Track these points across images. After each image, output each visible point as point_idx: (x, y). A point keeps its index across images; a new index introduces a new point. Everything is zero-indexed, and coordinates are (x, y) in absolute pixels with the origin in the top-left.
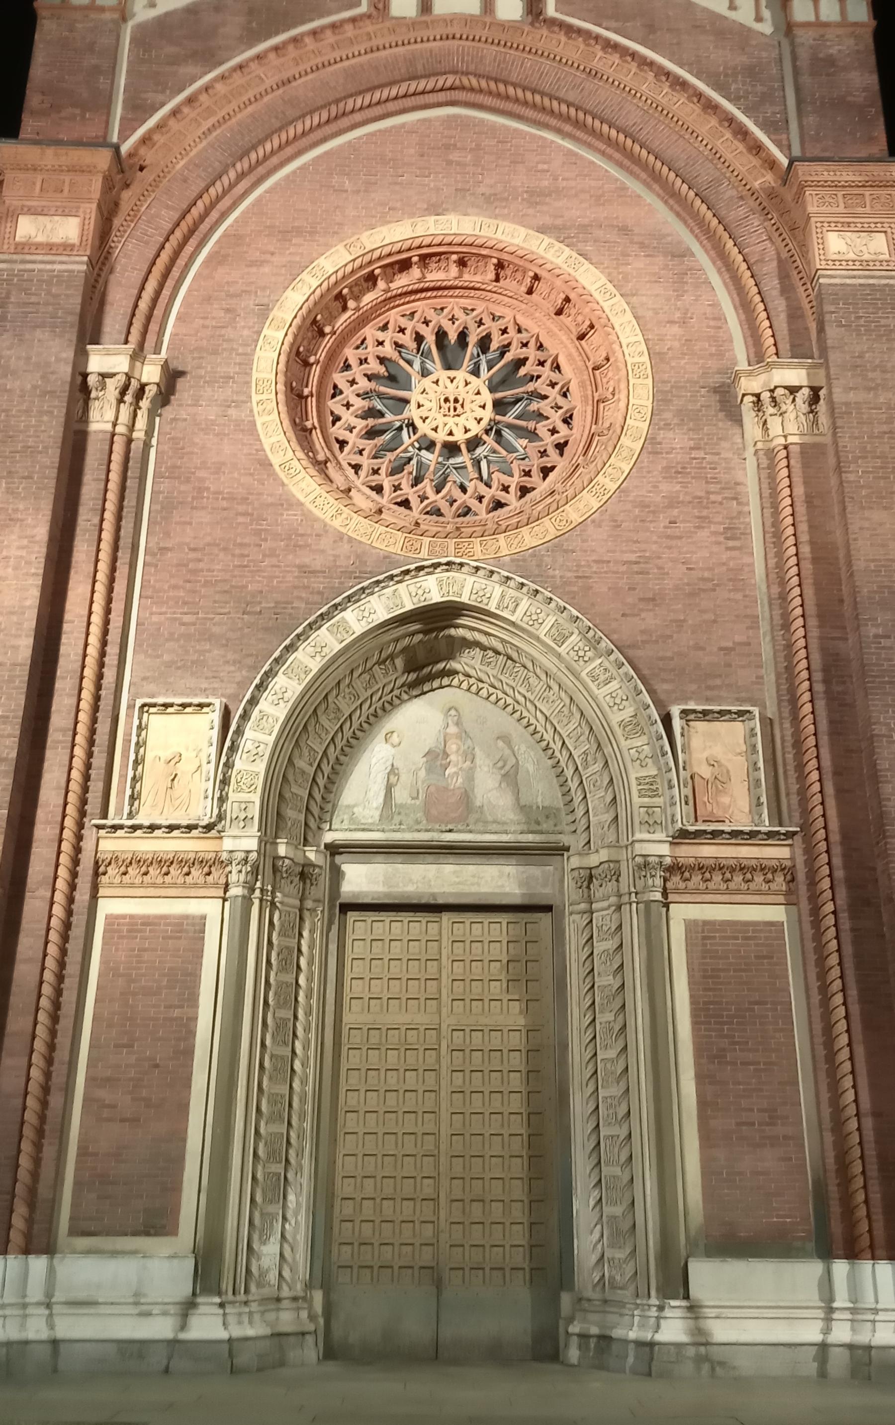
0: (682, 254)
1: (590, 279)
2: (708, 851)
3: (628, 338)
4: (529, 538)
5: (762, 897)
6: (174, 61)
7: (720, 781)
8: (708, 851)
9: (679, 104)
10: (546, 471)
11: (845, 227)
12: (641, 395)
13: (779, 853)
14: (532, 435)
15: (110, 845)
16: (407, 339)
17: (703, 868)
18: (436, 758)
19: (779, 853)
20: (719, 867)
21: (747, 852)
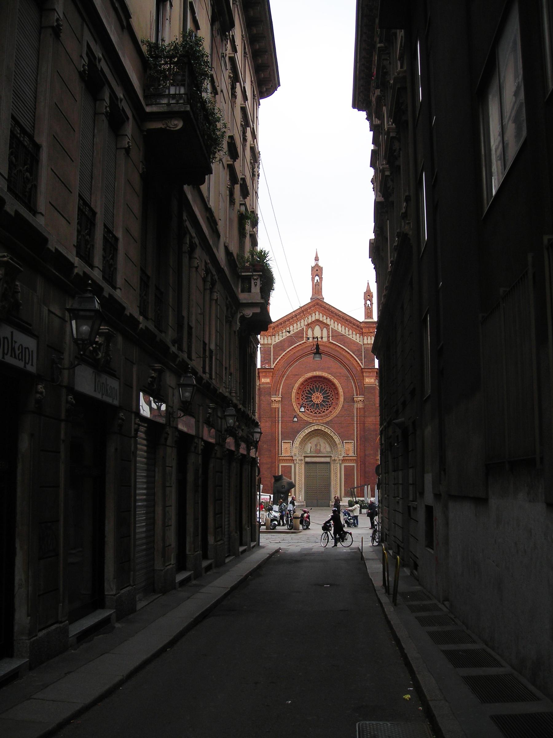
0: (348, 377)
1: (336, 381)
2: (347, 458)
3: (341, 390)
4: (328, 420)
5: (353, 463)
6: (279, 350)
7: (349, 450)
8: (347, 458)
9: (348, 356)
10: (330, 407)
11: (368, 377)
12: (342, 399)
13: (355, 458)
14: (328, 402)
15: (280, 458)
16: (311, 387)
17: (346, 460)
18: (316, 445)
19: (355, 458)
20: (348, 460)
21: (351, 458)
